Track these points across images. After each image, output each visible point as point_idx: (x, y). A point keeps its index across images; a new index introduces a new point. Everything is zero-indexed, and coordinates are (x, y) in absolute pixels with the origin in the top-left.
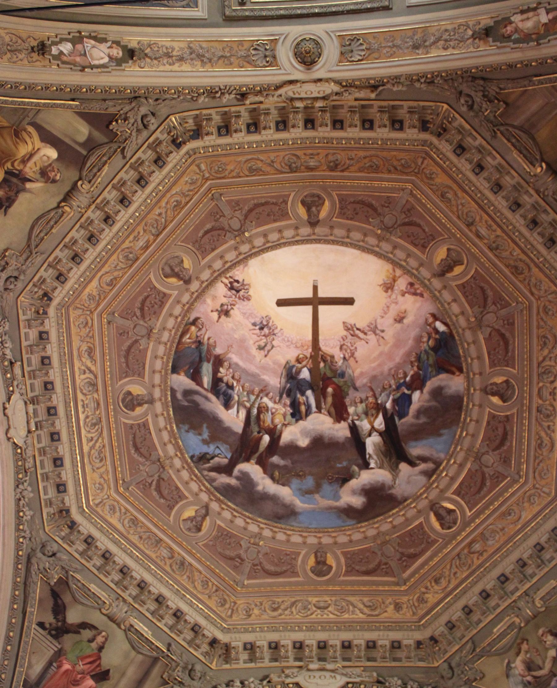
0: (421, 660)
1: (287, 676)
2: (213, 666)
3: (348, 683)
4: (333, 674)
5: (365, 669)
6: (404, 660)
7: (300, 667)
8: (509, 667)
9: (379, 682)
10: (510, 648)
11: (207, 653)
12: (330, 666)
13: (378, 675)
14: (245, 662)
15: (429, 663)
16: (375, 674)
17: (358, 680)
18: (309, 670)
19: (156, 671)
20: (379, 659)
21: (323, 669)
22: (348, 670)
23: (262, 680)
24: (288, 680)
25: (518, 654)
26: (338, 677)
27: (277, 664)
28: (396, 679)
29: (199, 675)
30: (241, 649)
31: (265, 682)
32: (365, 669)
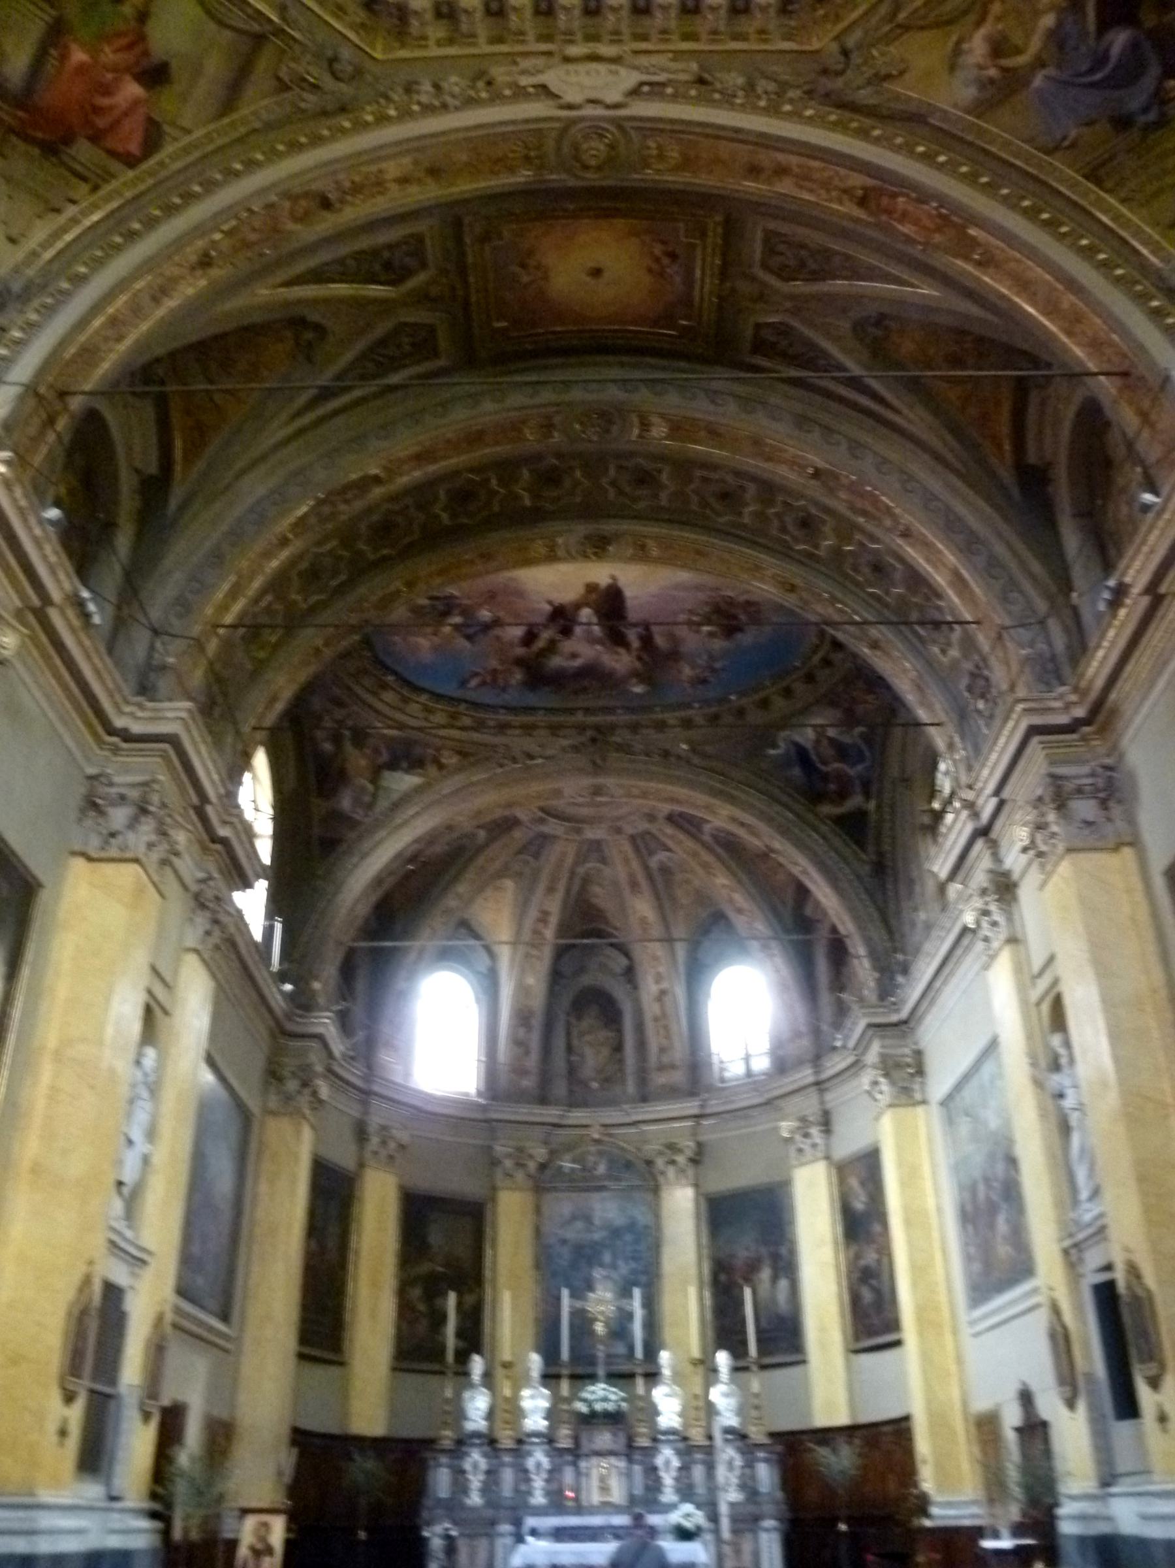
0: (788, 37)
1: (524, 72)
2: (378, 55)
3: (642, 84)
4: (613, 67)
5: (678, 55)
6: (753, 37)
7: (549, 54)
8: (957, 51)
9: (701, 81)
10: (965, 13)
11: (363, 25)
12: (605, 50)
13: (701, 67)
14: (439, 43)
15: (802, 43)
16: (694, 66)
17: (661, 77)
18: (567, 60)
19: (264, 63)
20: (704, 36)
21: (594, 58)
22: (644, 60)
23: (474, 79)
24: (524, 81)
25: (979, 24)
26: (623, 71)
27: (504, 48)
28: (733, 74)
29: (350, 69)
30: (429, 16)
31: (480, 84)
32: (678, 55)
